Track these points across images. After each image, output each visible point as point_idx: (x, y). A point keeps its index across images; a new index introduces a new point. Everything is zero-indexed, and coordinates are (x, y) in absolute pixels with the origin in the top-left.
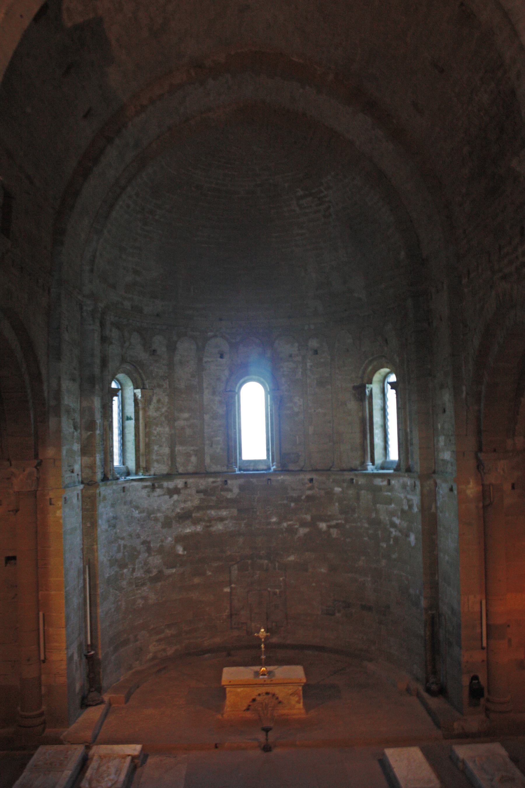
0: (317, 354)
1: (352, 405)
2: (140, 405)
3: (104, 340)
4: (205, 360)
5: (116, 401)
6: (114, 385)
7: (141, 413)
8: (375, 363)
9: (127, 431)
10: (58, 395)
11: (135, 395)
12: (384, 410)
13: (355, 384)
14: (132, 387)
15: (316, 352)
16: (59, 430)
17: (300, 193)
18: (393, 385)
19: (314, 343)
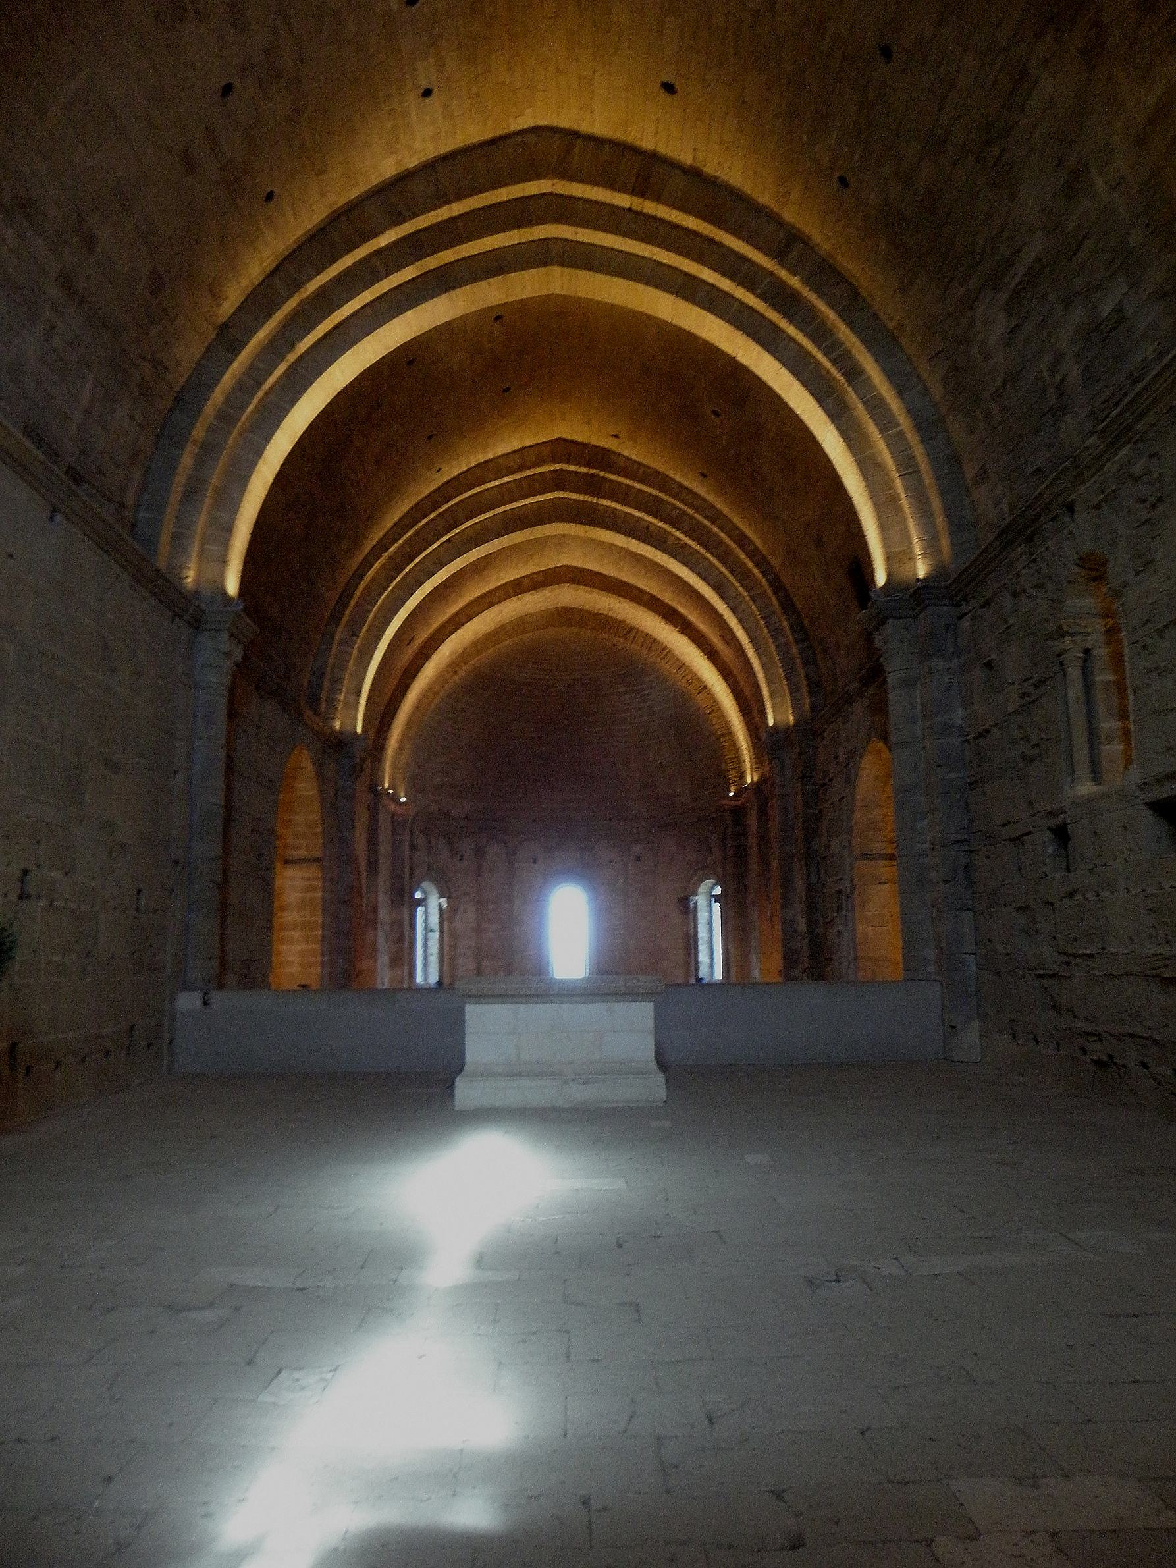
0: (639, 861)
1: (676, 918)
2: (445, 916)
3: (413, 846)
4: (517, 865)
5: (420, 910)
6: (418, 895)
7: (446, 924)
8: (700, 873)
9: (430, 943)
10: (375, 911)
11: (440, 904)
12: (710, 923)
13: (679, 896)
14: (437, 895)
15: (638, 859)
16: (375, 944)
17: (622, 689)
18: (717, 899)
19: (636, 849)
